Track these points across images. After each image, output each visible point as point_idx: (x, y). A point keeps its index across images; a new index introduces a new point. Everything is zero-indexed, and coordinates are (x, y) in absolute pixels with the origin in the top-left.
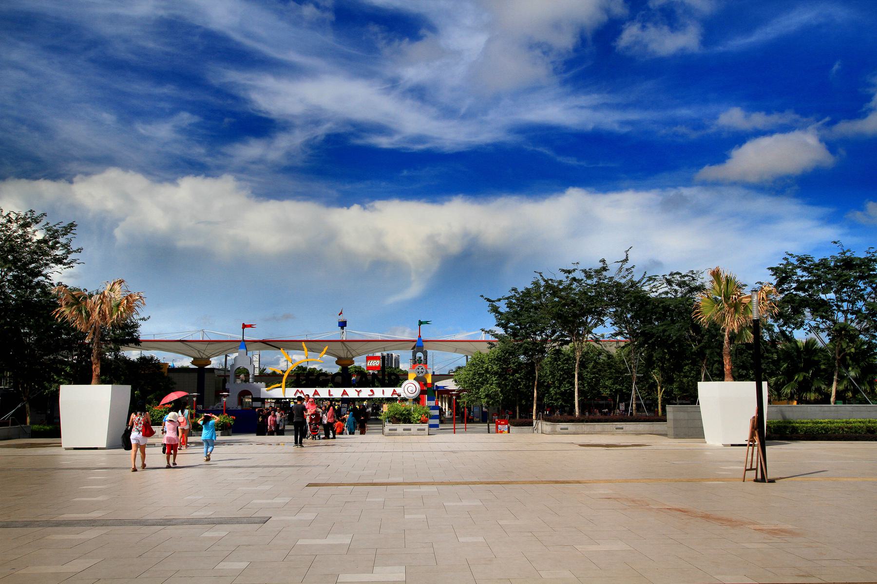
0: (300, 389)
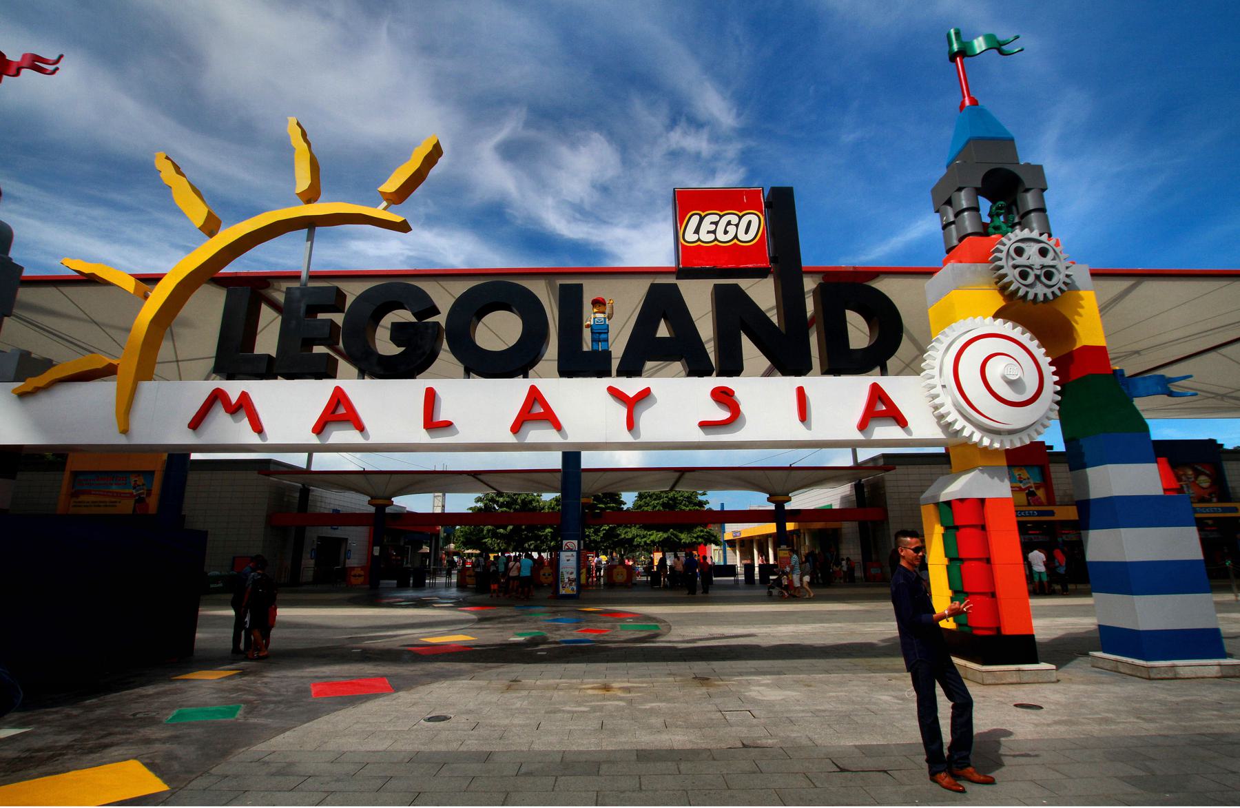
0: (234, 389)
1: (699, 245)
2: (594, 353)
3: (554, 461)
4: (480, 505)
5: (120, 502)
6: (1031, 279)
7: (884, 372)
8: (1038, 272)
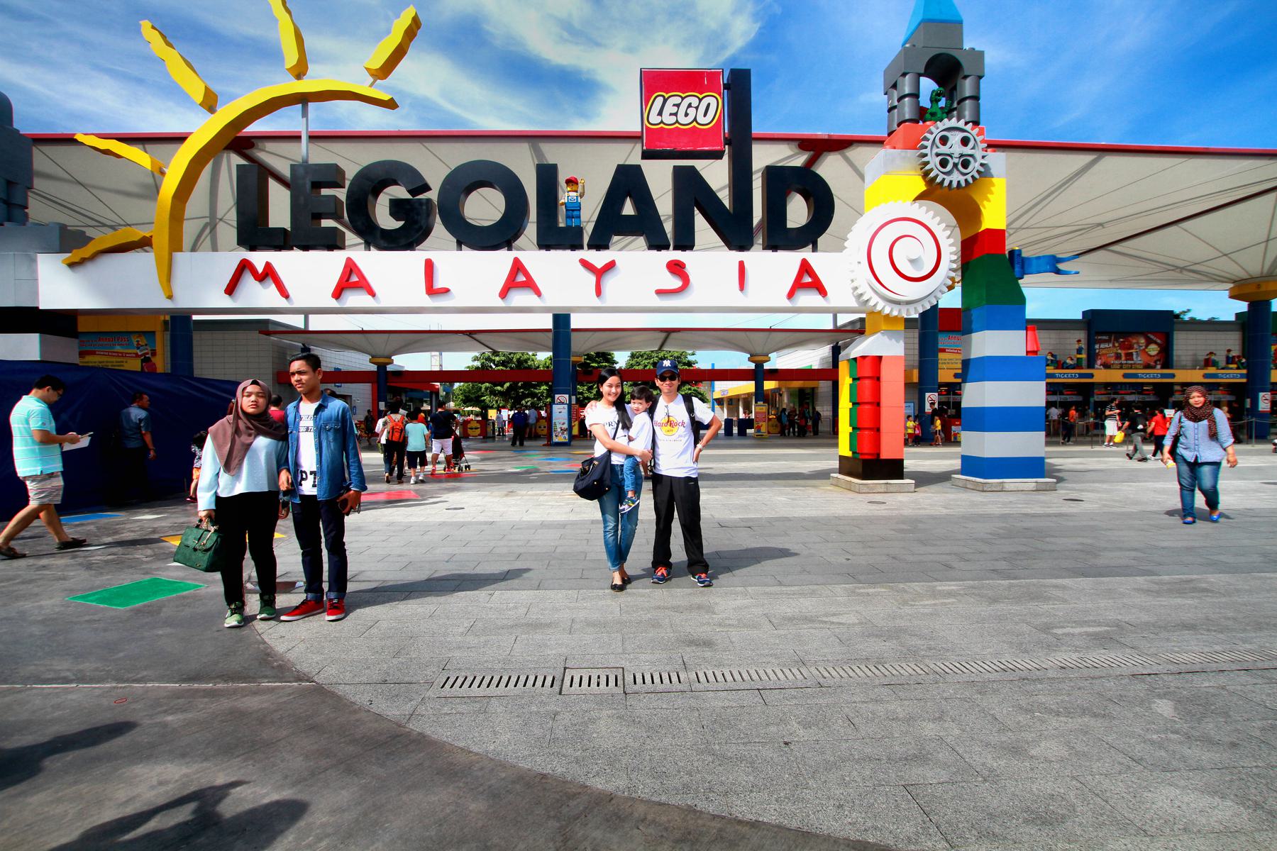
0: (259, 259)
1: (662, 127)
2: (568, 228)
3: (546, 322)
4: (478, 364)
5: (126, 362)
6: (949, 167)
7: (815, 249)
8: (956, 161)
